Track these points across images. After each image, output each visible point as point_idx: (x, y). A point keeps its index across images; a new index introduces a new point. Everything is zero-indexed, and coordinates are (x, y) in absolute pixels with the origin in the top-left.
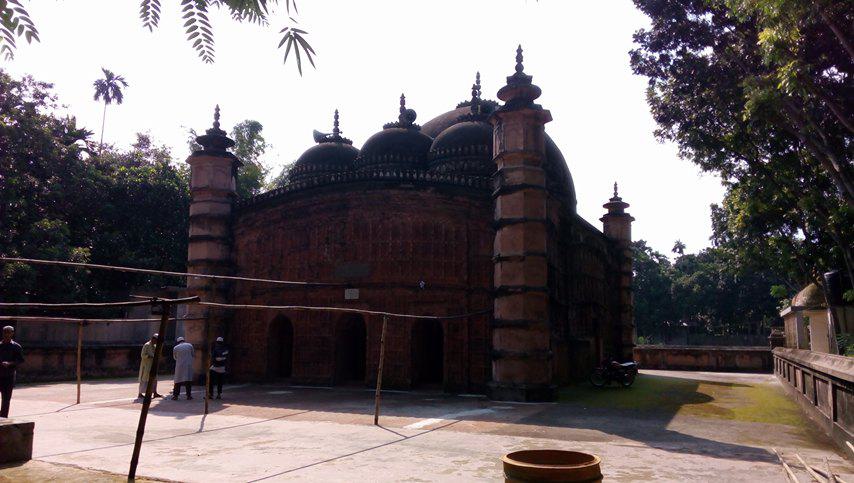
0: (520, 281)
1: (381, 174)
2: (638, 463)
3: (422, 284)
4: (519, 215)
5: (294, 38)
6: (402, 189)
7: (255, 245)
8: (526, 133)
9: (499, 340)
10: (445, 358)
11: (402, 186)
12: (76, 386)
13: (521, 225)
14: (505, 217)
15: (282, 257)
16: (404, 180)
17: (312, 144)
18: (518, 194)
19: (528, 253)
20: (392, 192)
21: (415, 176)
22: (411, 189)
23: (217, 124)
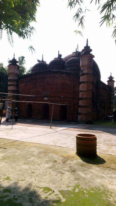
0: (85, 96)
2: (109, 138)
3: (62, 97)
4: (86, 81)
5: (31, 47)
6: (58, 74)
8: (88, 60)
9: (80, 110)
10: (67, 114)
11: (58, 73)
13: (86, 83)
16: (59, 72)
17: (38, 62)
18: (86, 76)
19: (87, 90)
21: (61, 71)
22: (60, 74)
23: (14, 58)
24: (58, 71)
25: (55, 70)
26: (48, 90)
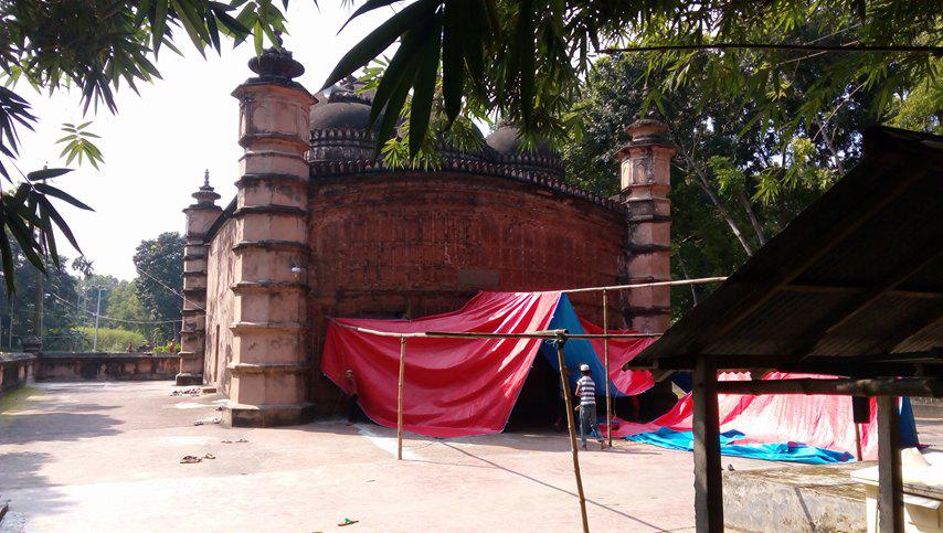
1: (514, 174)
6: (538, 194)
7: (342, 230)
14: (657, 244)
15: (383, 250)
16: (538, 185)
20: (528, 196)
22: (547, 197)
24: (535, 179)
25: (521, 175)
26: (490, 263)
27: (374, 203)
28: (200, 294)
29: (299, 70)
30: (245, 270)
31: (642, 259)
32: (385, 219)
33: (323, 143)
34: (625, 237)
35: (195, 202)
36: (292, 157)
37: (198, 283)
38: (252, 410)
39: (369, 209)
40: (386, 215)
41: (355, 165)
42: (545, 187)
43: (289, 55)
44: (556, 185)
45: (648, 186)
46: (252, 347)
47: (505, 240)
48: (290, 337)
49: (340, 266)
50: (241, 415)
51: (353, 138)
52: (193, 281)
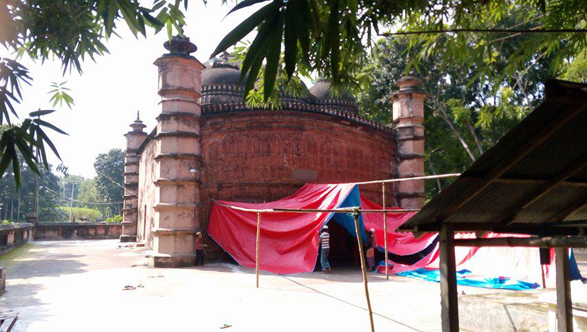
7: (221, 146)
12: (255, 275)
14: (415, 153)
15: (246, 158)
16: (342, 118)
20: (335, 125)
22: (347, 125)
24: (340, 114)
26: (312, 166)
27: (241, 130)
28: (134, 186)
29: (194, 48)
30: (162, 171)
31: (406, 163)
32: (246, 139)
33: (209, 93)
34: (396, 149)
35: (131, 130)
36: (190, 102)
37: (133, 179)
38: (167, 257)
39: (237, 134)
40: (248, 137)
41: (228, 106)
42: (346, 119)
43: (188, 39)
44: (353, 118)
45: (410, 118)
46: (166, 218)
47: (321, 151)
48: (190, 212)
49: (220, 168)
50: (159, 260)
51: (227, 90)
52: (131, 178)
